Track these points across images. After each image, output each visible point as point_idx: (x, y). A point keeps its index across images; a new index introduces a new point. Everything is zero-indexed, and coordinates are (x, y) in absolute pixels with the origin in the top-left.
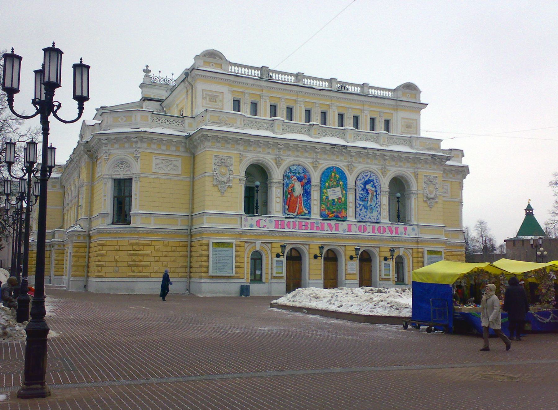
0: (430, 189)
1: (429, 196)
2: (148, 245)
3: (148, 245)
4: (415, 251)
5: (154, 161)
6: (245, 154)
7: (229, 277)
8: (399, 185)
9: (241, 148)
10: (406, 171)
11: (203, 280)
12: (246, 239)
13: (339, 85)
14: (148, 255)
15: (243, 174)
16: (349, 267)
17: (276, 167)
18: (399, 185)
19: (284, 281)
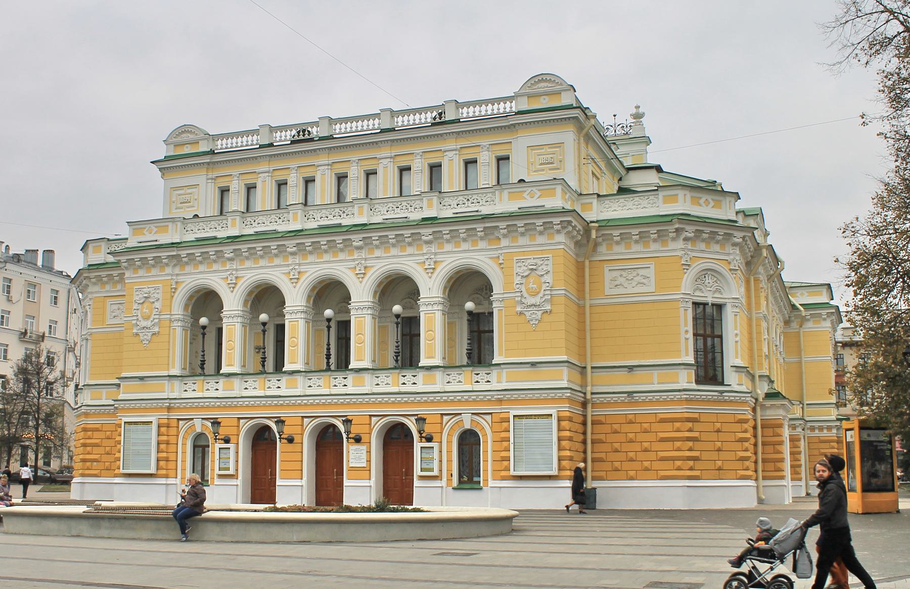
0: (531, 286)
1: (531, 300)
2: (97, 430)
3: (97, 430)
4: (496, 418)
5: (109, 308)
6: (181, 279)
7: (151, 475)
8: (468, 284)
9: (177, 270)
10: (479, 257)
11: (117, 480)
12: (175, 415)
13: (435, 113)
14: (97, 445)
15: (178, 309)
16: (351, 456)
17: (228, 291)
18: (468, 284)
19: (239, 482)
